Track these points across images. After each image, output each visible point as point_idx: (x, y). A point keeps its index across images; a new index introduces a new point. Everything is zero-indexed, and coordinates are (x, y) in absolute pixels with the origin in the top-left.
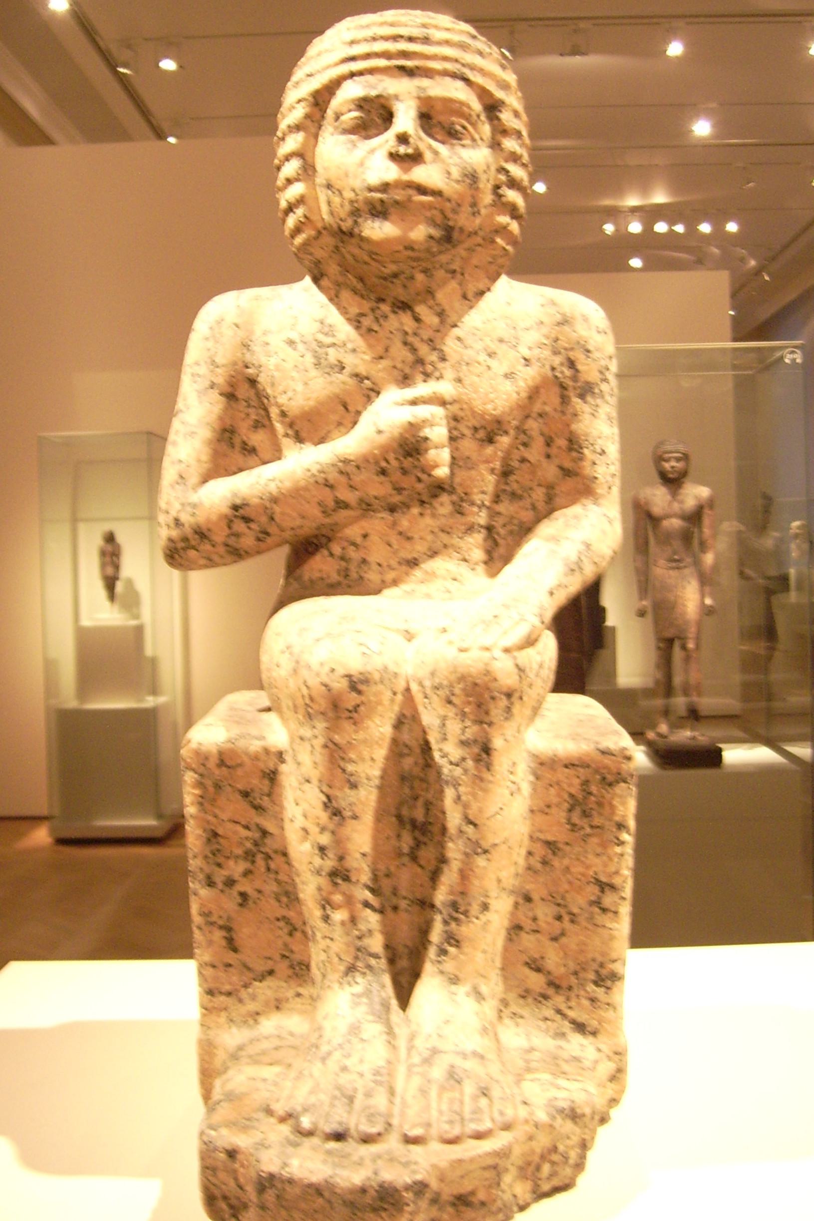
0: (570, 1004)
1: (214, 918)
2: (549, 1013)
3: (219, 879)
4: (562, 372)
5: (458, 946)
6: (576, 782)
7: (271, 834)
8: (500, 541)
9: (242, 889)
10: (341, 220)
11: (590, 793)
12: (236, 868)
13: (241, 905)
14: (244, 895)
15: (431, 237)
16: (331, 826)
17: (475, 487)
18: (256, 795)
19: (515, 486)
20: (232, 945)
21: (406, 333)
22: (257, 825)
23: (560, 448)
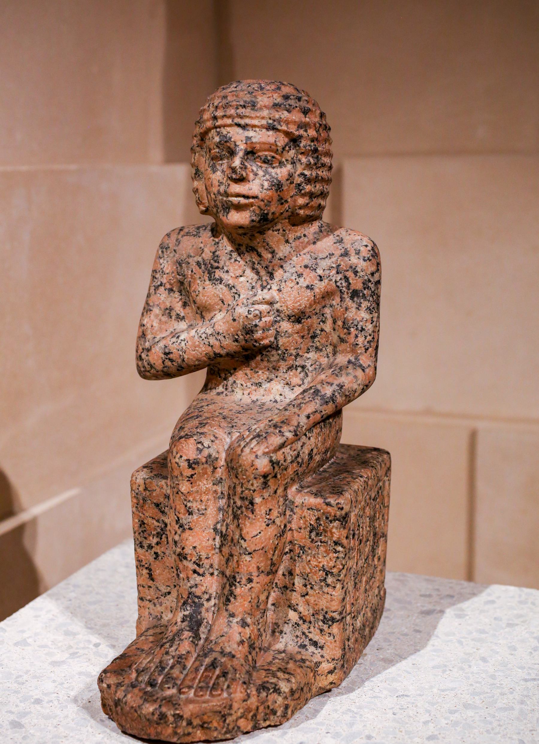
0: (310, 630)
1: (143, 563)
2: (299, 633)
3: (145, 546)
4: (341, 284)
5: (235, 598)
6: (314, 518)
8: (310, 374)
9: (156, 551)
11: (320, 525)
13: (155, 558)
14: (156, 553)
15: (253, 221)
16: (179, 532)
17: (292, 346)
18: (162, 505)
19: (318, 344)
20: (151, 577)
21: (254, 263)
22: (163, 521)
23: (339, 326)
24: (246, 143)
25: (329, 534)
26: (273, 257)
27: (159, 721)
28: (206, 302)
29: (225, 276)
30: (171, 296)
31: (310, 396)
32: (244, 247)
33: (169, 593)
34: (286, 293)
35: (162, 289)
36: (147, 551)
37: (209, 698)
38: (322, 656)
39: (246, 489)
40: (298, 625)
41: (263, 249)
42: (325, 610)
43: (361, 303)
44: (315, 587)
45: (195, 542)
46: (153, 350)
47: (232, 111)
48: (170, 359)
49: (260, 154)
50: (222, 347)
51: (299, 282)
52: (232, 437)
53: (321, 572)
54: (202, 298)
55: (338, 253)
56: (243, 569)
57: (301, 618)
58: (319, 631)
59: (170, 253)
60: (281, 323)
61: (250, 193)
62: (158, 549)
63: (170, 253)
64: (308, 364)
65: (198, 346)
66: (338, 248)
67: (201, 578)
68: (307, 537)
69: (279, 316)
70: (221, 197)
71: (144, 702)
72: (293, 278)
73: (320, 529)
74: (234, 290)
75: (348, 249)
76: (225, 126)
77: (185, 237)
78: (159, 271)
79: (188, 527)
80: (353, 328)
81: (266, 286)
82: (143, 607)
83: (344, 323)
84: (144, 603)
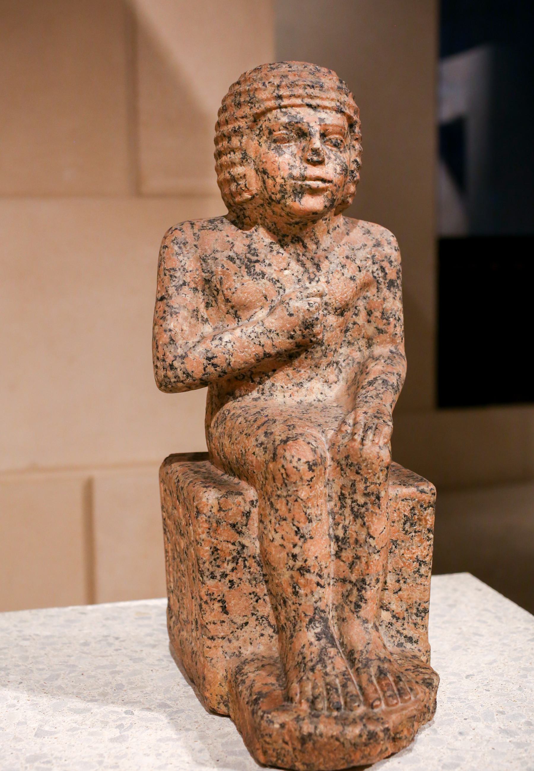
0: (404, 627)
1: (215, 596)
2: (393, 633)
3: (218, 574)
4: (378, 274)
5: (366, 603)
7: (247, 547)
8: (343, 370)
9: (231, 579)
10: (273, 193)
12: (228, 567)
13: (230, 588)
18: (239, 525)
19: (350, 338)
21: (298, 255)
22: (240, 542)
24: (320, 125)
25: (424, 522)
26: (317, 248)
27: (368, 742)
28: (246, 299)
29: (267, 270)
30: (196, 296)
31: (381, 387)
32: (290, 237)
33: (247, 624)
34: (335, 284)
35: (186, 289)
36: (220, 581)
37: (402, 704)
38: (419, 650)
39: (372, 483)
40: (391, 625)
41: (309, 239)
42: (419, 602)
43: (396, 293)
44: (408, 581)
45: (316, 551)
46: (191, 356)
47: (301, 91)
48: (213, 365)
49: (332, 137)
50: (274, 346)
51: (345, 273)
52: (326, 436)
53: (415, 563)
54: (241, 295)
55: (370, 243)
56: (373, 569)
57: (394, 616)
58: (413, 626)
59: (190, 248)
60: (328, 316)
61: (328, 177)
62: (233, 576)
63: (190, 248)
64: (341, 359)
65: (248, 347)
66: (368, 239)
67: (323, 590)
68: (401, 529)
69: (326, 309)
70: (293, 182)
71: (343, 727)
72: (339, 269)
73: (415, 519)
74: (278, 285)
75: (380, 240)
76: (292, 106)
77: (203, 231)
78: (179, 269)
79: (309, 536)
80: (392, 317)
81: (314, 279)
82: (215, 646)
83: (383, 313)
84: (215, 642)
